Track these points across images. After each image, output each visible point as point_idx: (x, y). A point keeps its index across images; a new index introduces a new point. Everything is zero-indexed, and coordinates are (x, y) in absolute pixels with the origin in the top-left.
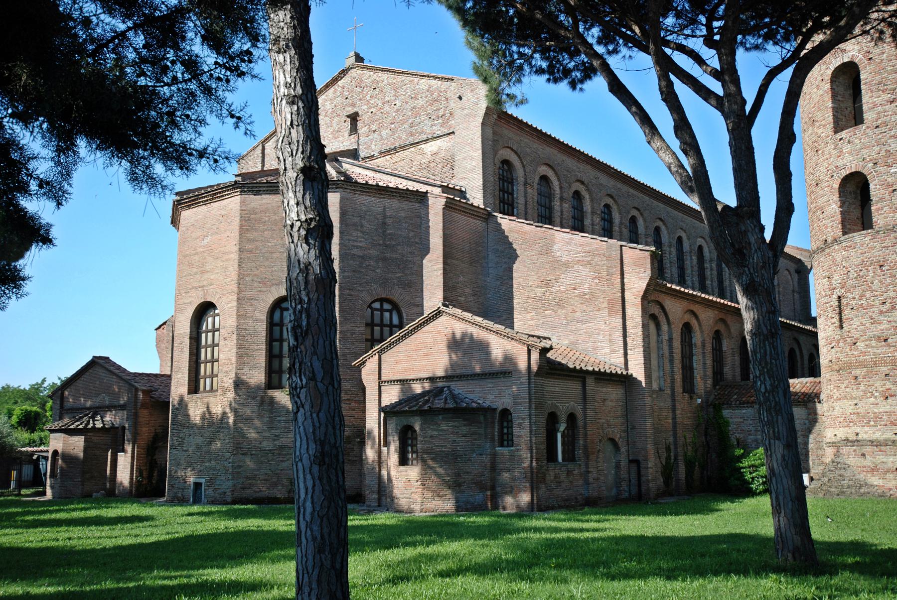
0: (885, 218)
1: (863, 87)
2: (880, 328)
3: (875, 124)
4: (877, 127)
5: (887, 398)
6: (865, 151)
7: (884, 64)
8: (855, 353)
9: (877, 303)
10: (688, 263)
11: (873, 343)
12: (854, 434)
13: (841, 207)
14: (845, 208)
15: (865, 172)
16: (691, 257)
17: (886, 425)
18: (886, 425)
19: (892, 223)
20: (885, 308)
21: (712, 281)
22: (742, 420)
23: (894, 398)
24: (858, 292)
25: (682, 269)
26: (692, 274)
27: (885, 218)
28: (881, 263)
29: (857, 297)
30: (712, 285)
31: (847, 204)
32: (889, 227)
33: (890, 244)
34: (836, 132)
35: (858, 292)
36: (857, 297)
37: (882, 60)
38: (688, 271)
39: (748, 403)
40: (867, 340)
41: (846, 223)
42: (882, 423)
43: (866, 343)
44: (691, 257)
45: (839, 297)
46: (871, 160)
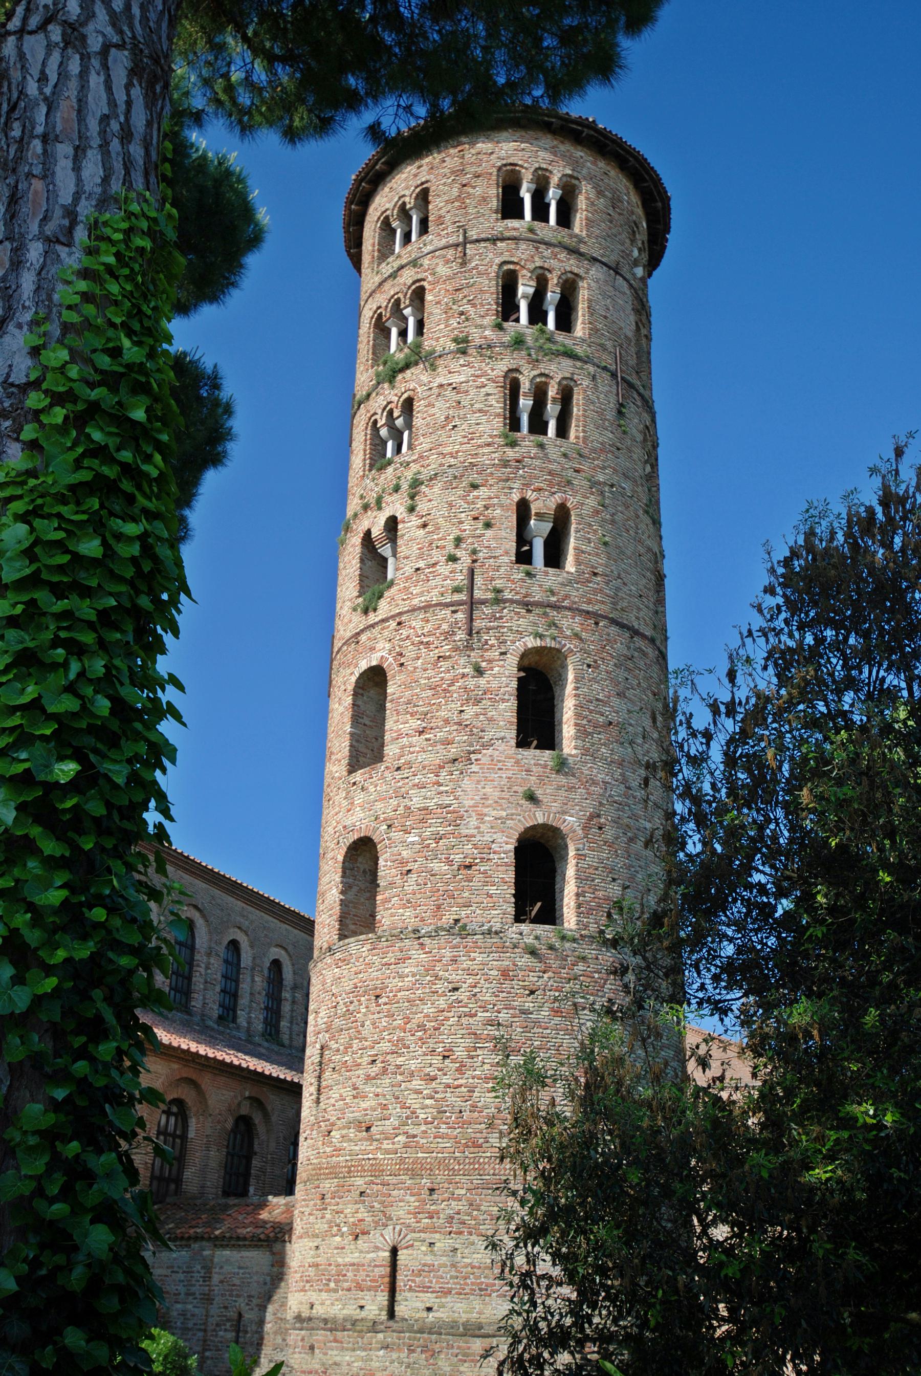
0: (392, 915)
1: (388, 705)
2: (364, 1105)
3: (396, 764)
4: (398, 769)
5: (357, 1237)
6: (379, 805)
7: (419, 673)
8: (328, 1150)
9: (366, 1060)
10: (245, 987)
11: (352, 1133)
12: (309, 1306)
13: (342, 893)
14: (351, 895)
15: (376, 839)
16: (253, 977)
17: (349, 1290)
18: (349, 1290)
19: (400, 925)
20: (374, 1070)
21: (291, 1023)
22: (168, 1272)
23: (366, 1237)
24: (343, 1038)
25: (230, 996)
26: (250, 1007)
27: (392, 915)
28: (378, 992)
29: (342, 1048)
30: (290, 1028)
31: (355, 889)
32: (395, 932)
33: (393, 960)
34: (350, 772)
35: (343, 1038)
36: (342, 1048)
37: (415, 668)
38: (243, 1001)
39: (182, 1238)
40: (344, 1128)
41: (348, 921)
42: (346, 1285)
43: (344, 1132)
44: (253, 977)
45: (322, 1048)
46: (385, 820)
